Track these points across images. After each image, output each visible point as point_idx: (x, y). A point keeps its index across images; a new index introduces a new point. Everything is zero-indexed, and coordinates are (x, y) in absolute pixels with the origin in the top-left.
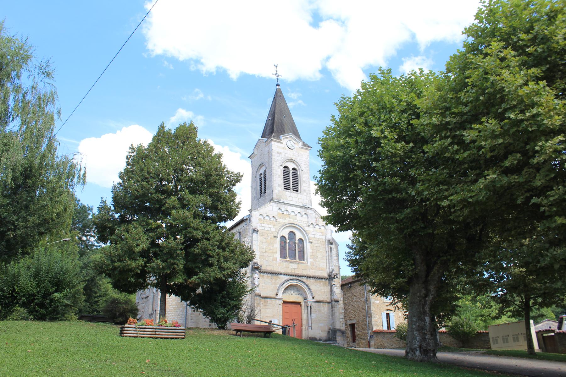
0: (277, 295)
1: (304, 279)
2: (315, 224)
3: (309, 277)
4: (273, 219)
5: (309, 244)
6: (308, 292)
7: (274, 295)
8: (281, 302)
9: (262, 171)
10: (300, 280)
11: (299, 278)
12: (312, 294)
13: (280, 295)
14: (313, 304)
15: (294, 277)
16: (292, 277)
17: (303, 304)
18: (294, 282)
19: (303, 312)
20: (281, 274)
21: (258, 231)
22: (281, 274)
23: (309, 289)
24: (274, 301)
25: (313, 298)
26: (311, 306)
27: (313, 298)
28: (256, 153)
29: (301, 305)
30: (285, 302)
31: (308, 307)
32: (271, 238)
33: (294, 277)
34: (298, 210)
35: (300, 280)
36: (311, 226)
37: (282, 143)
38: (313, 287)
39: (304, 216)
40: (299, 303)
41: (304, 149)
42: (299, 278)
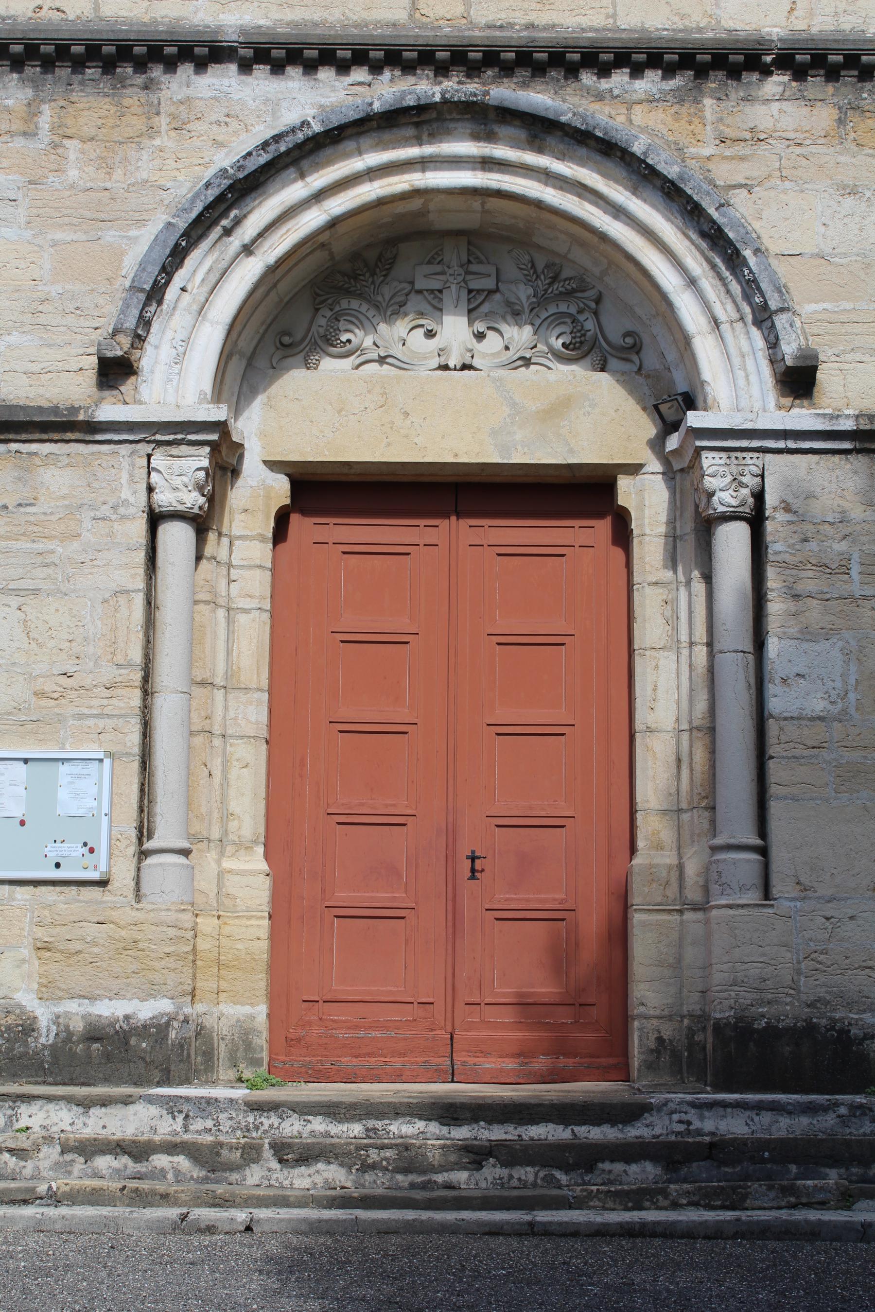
0: (115, 371)
1: (637, 109)
7: (70, 386)
10: (540, 129)
11: (538, 97)
12: (763, 317)
13: (179, 376)
14: (781, 474)
15: (424, 88)
16: (388, 90)
17: (647, 499)
18: (452, 167)
19: (651, 628)
20: (202, 52)
22: (202, 52)
23: (723, 246)
24: (57, 472)
25: (798, 381)
26: (756, 519)
27: (798, 381)
29: (622, 533)
30: (320, 491)
31: (706, 526)
33: (424, 88)
35: (540, 129)
38: (780, 219)
40: (587, 493)
42: (538, 97)
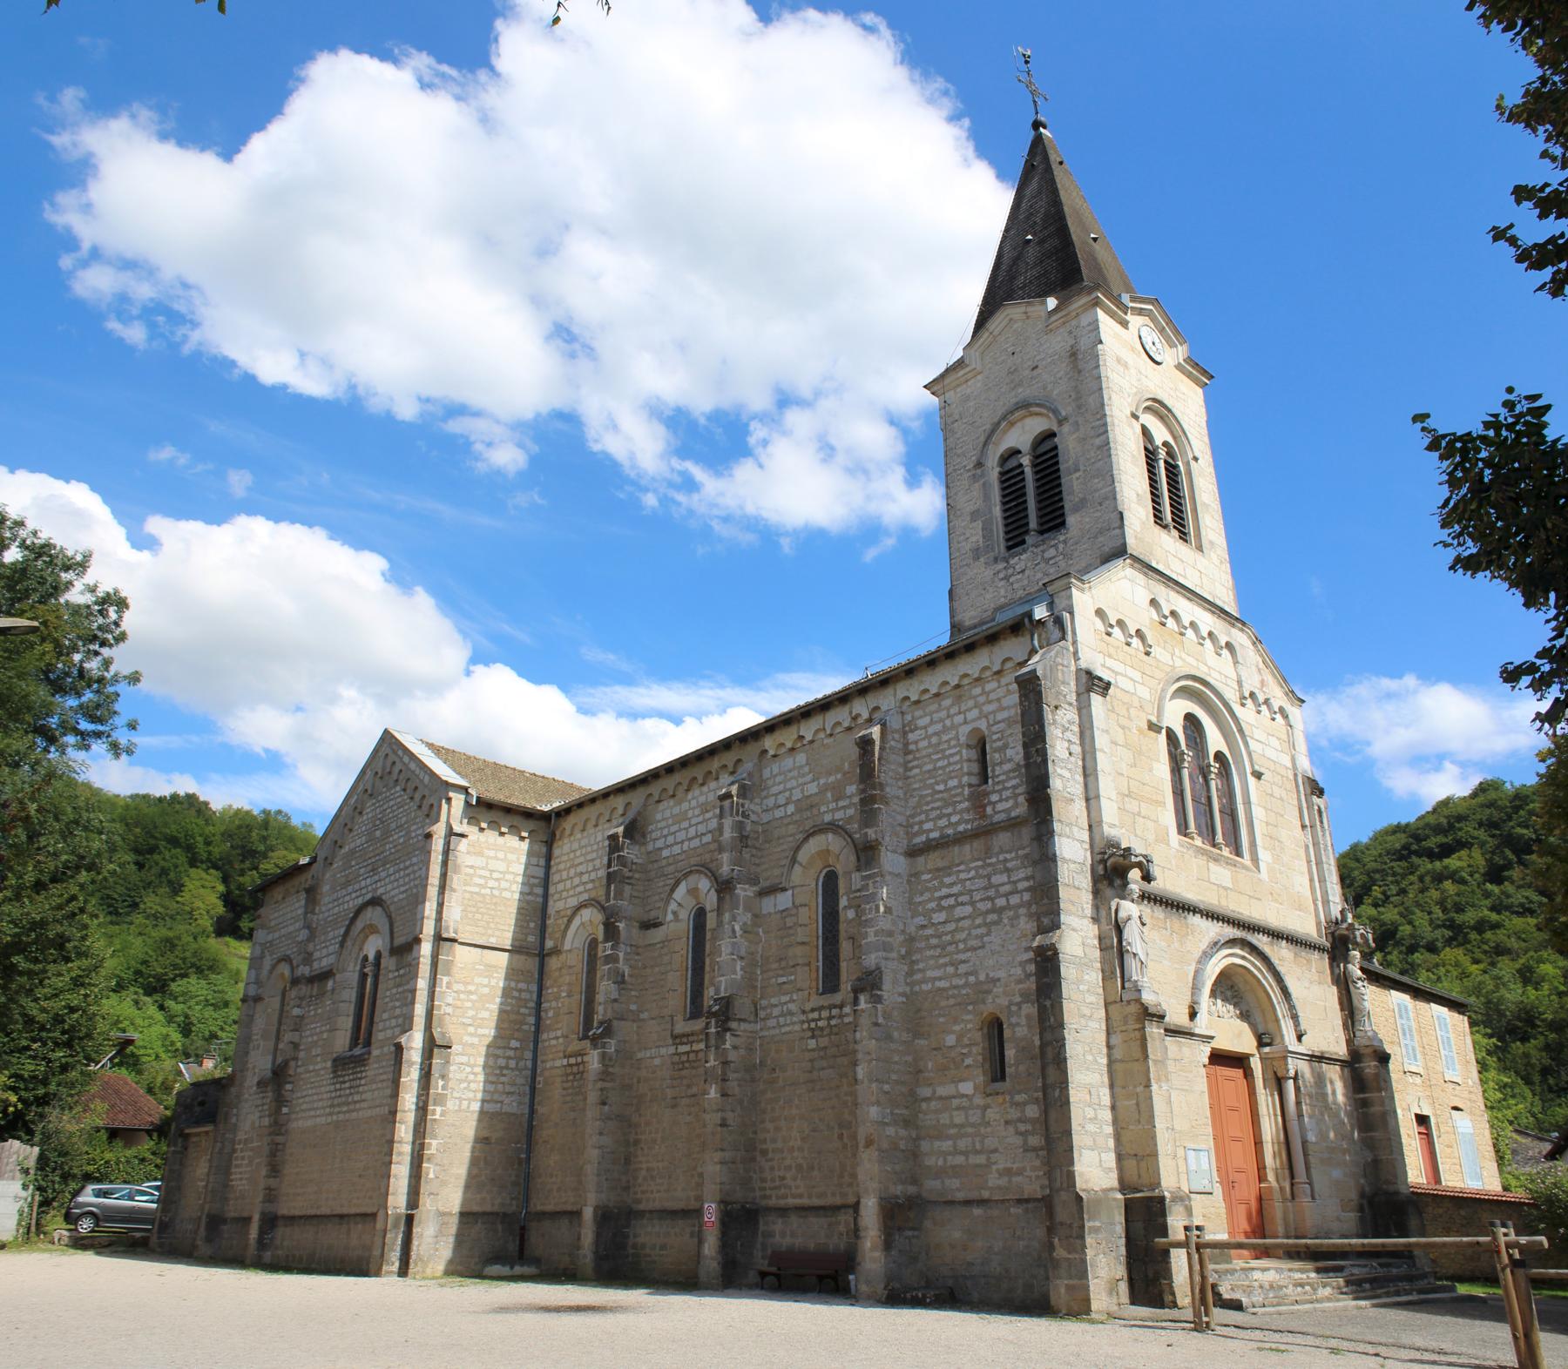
2: (1261, 699)
3: (1276, 935)
4: (1135, 642)
5: (1251, 780)
6: (1281, 1010)
8: (1206, 1051)
9: (1021, 436)
17: (1256, 1064)
21: (1108, 684)
25: (1299, 1038)
28: (975, 363)
32: (1140, 731)
34: (1207, 621)
36: (1249, 702)
37: (1125, 324)
39: (1225, 652)
41: (1189, 375)
